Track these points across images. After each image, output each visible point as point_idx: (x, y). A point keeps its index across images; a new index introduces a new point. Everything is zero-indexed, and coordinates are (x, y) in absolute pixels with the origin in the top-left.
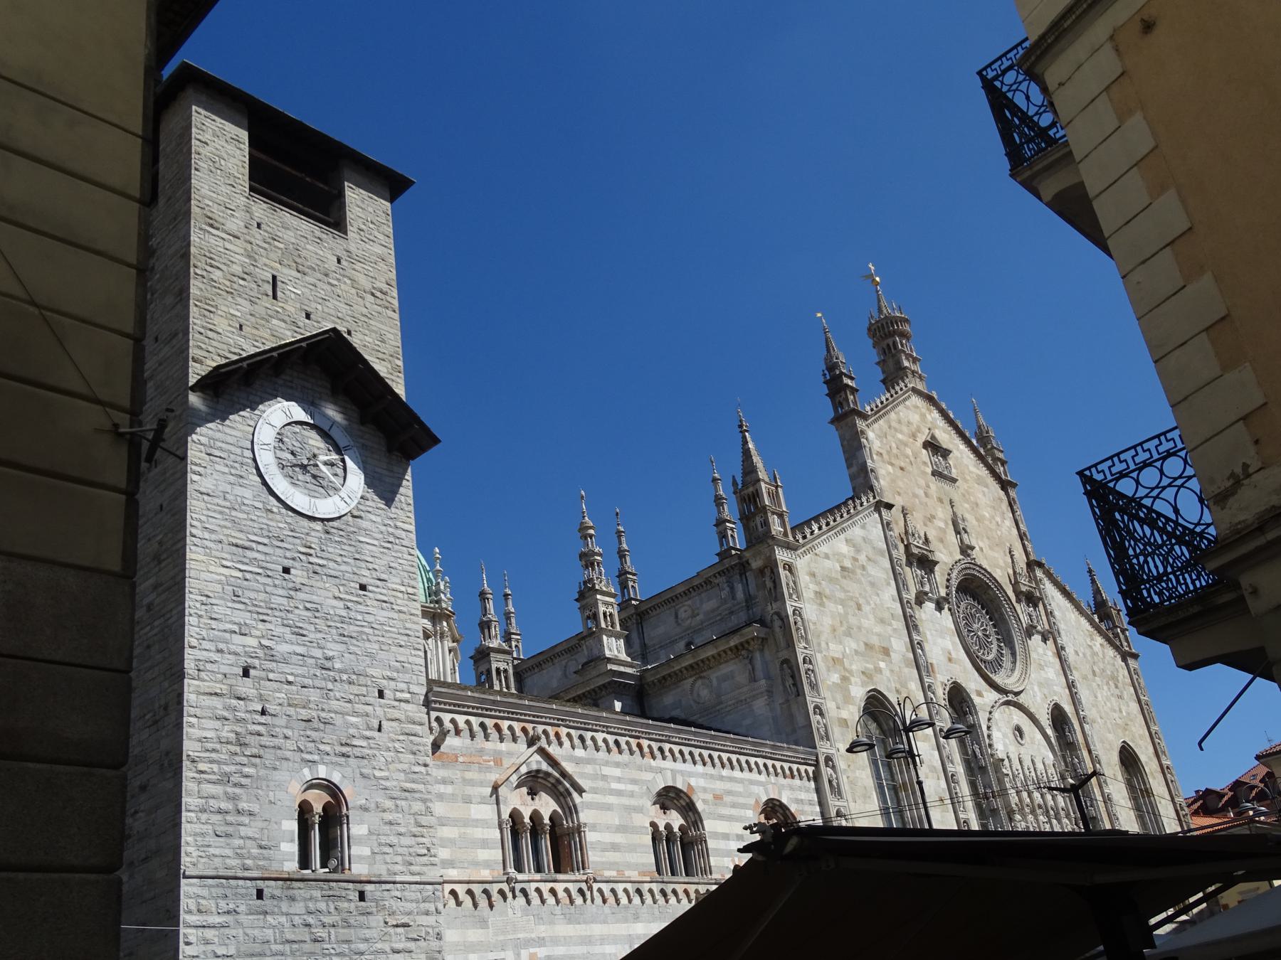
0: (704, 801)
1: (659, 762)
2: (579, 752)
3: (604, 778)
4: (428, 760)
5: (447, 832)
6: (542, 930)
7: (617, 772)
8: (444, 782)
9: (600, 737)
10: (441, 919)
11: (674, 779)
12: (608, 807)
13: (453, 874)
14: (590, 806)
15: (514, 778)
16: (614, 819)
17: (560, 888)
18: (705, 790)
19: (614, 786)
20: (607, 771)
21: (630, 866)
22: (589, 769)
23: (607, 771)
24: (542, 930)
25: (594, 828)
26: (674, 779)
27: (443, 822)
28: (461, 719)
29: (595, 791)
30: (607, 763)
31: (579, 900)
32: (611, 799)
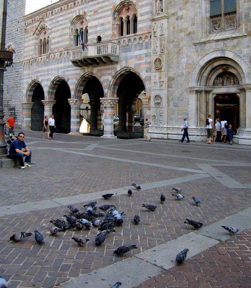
0: (90, 16)
1: (75, 9)
2: (53, 17)
3: (58, 22)
4: (23, 34)
5: (26, 49)
6: (40, 69)
7: (62, 18)
8: (27, 38)
9: (56, 9)
10: (22, 70)
11: (79, 12)
12: (58, 30)
13: (26, 59)
14: (54, 32)
15: (37, 32)
16: (58, 34)
17: (43, 57)
18: (91, 11)
19: (60, 23)
20: (59, 19)
21: (61, 47)
22: (54, 21)
23: (59, 19)
24: (40, 69)
25: (53, 38)
26: (79, 12)
27: (25, 47)
28: (29, 21)
29: (55, 27)
30: (59, 17)
31: (47, 60)
32: (59, 28)
